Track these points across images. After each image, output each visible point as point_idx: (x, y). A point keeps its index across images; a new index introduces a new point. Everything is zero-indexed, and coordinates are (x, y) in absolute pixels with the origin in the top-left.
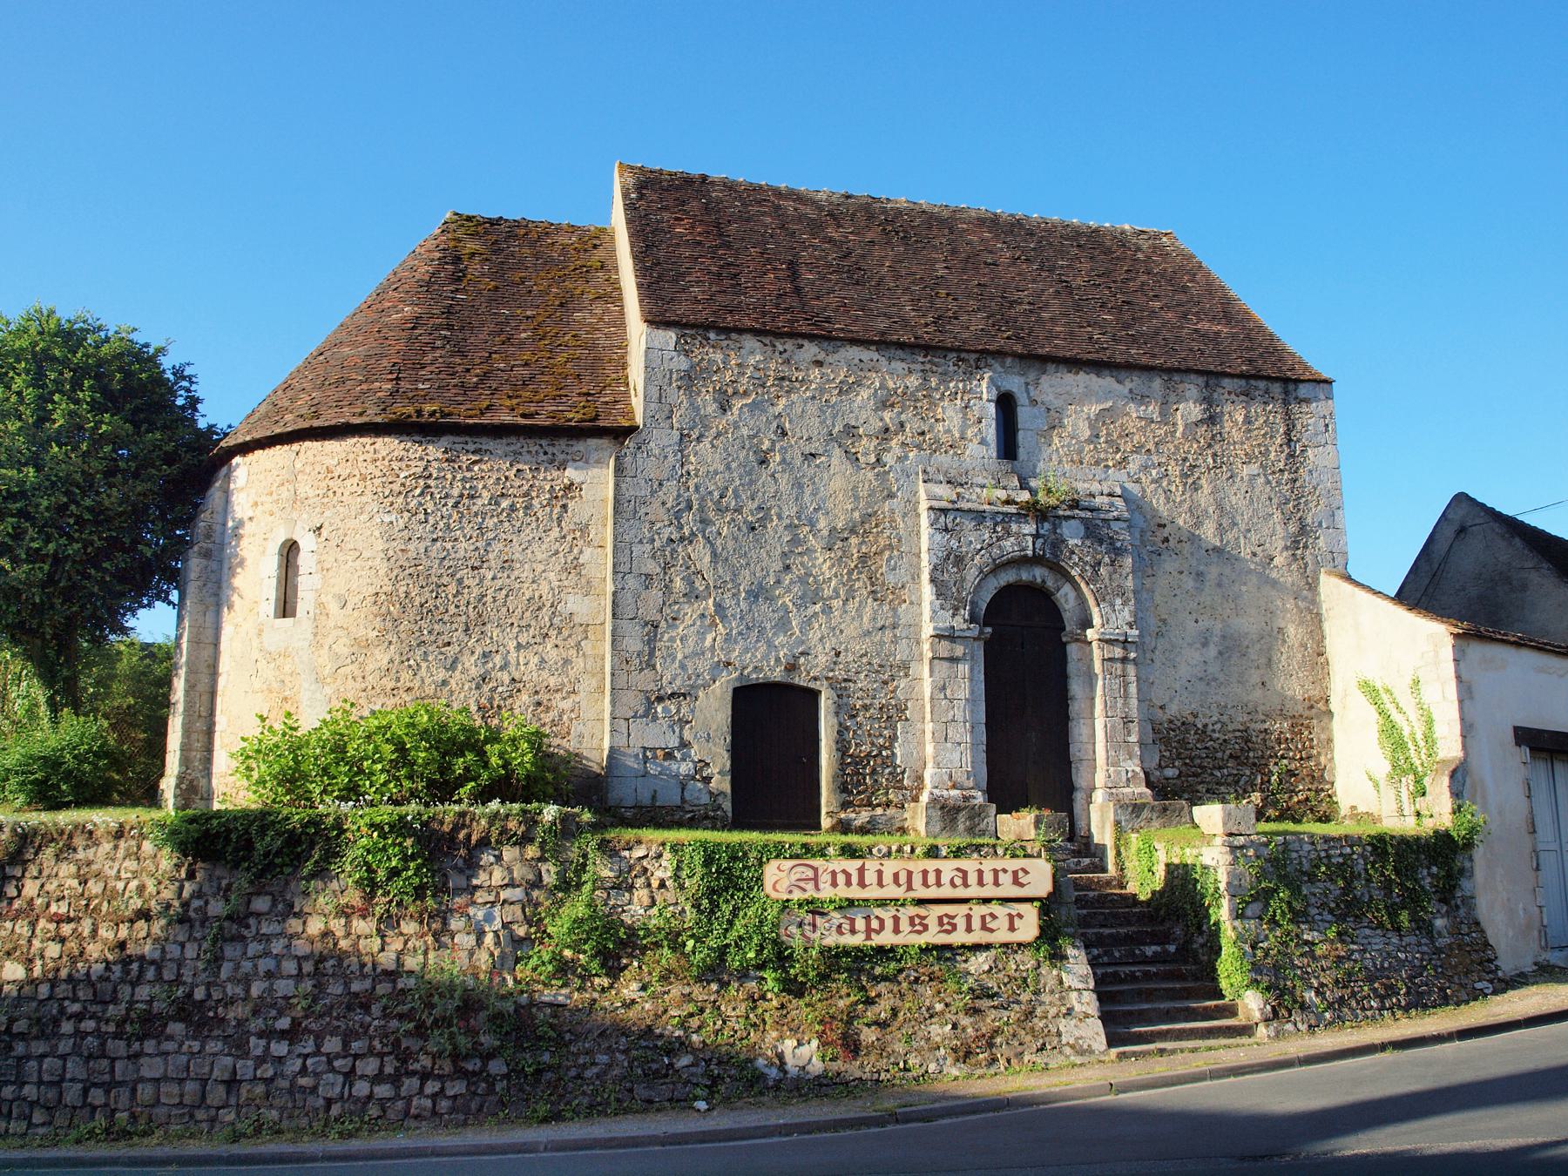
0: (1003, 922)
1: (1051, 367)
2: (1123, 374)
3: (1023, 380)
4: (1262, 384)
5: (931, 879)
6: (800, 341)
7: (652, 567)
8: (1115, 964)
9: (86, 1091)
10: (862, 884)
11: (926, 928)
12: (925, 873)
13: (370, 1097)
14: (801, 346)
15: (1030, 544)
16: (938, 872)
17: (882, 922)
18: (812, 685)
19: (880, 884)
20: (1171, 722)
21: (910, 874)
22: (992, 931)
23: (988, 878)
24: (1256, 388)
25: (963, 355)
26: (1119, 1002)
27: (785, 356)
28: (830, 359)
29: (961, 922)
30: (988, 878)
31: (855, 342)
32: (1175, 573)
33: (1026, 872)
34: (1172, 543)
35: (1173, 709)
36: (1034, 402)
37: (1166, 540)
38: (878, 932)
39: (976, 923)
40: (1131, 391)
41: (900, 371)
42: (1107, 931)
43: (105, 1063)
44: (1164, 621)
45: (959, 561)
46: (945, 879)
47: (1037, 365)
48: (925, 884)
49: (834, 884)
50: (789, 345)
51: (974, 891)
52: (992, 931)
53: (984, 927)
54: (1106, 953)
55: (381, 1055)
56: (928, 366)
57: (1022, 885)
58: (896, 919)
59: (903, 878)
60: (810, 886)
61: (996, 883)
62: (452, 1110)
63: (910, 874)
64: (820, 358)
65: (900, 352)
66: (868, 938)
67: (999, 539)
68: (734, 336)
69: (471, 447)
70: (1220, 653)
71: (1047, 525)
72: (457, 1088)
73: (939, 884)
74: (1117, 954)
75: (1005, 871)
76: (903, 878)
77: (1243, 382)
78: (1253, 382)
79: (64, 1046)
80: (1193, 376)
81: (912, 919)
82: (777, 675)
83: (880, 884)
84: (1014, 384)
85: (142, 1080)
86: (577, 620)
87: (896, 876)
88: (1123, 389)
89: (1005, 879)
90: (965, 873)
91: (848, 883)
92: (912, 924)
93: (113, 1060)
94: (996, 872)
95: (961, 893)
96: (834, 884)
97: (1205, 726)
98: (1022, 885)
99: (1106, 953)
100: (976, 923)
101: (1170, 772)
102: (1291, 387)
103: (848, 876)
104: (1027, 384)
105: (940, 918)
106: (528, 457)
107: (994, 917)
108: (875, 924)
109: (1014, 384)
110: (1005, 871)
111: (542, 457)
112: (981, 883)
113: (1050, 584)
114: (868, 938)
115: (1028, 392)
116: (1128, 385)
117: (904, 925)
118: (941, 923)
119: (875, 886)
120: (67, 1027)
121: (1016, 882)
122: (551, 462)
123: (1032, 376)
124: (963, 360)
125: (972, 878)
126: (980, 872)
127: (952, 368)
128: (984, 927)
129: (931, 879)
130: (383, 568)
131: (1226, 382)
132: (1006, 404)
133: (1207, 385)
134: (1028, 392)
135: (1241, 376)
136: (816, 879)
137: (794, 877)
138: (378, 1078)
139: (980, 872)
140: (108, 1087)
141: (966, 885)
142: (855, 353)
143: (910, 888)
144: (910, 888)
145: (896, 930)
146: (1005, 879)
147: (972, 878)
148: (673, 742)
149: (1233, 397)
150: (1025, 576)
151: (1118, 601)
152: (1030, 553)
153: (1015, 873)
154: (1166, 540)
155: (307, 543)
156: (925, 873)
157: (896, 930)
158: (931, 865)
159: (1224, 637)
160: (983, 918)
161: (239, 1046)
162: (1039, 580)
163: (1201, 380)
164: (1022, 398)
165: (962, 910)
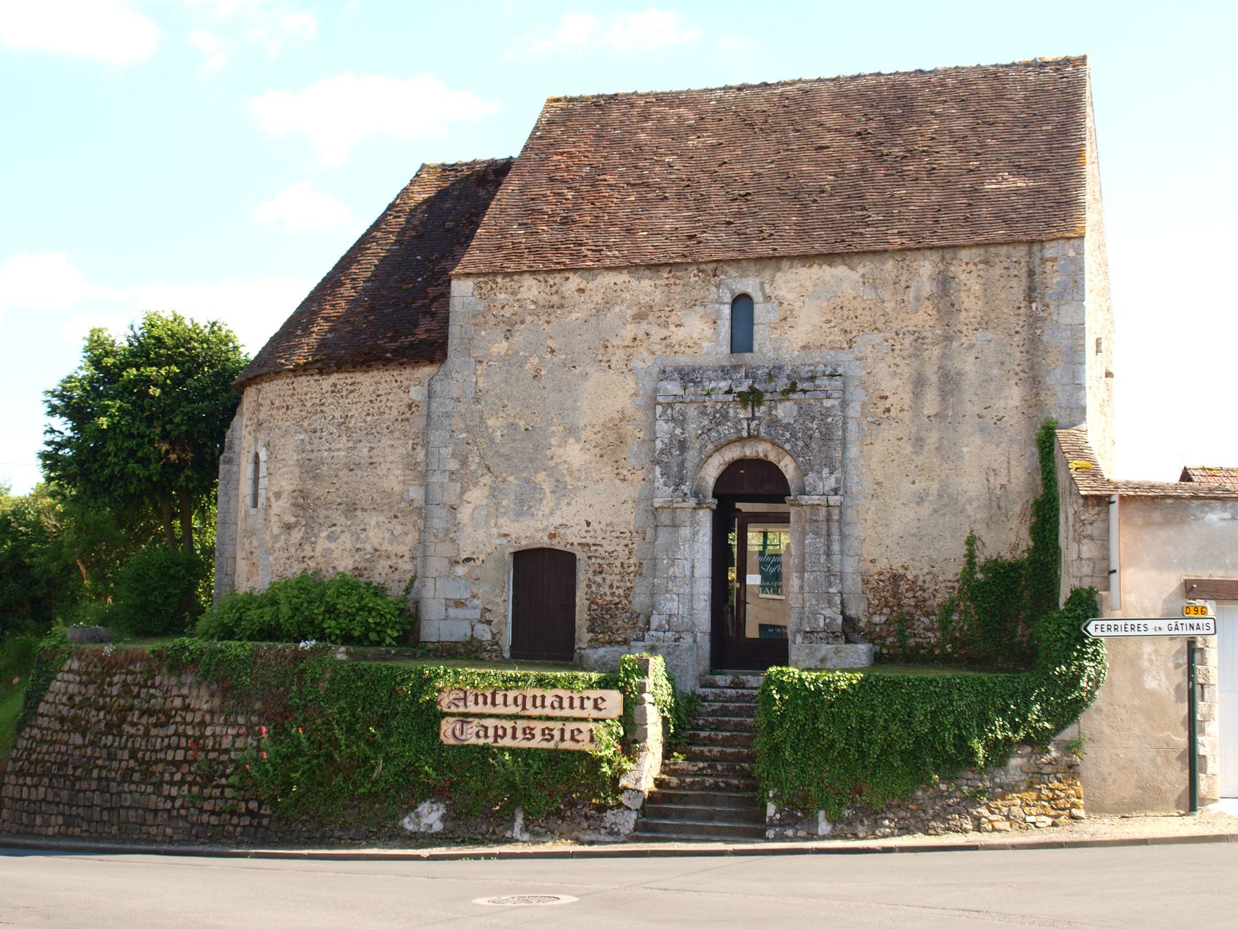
0: (585, 736)
1: (785, 264)
2: (856, 260)
3: (758, 281)
4: (1003, 250)
5: (539, 702)
6: (567, 274)
7: (454, 465)
8: (718, 776)
9: (101, 812)
10: (494, 704)
11: (533, 736)
12: (535, 697)
13: (208, 823)
14: (567, 279)
15: (745, 425)
16: (543, 697)
17: (505, 730)
18: (568, 549)
19: (505, 704)
20: (881, 574)
21: (525, 698)
22: (578, 741)
23: (577, 703)
24: (997, 255)
25: (703, 267)
26: (686, 804)
27: (554, 289)
28: (591, 285)
29: (557, 734)
30: (577, 703)
31: (609, 269)
32: (894, 441)
33: (603, 700)
34: (893, 413)
35: (882, 564)
36: (768, 298)
37: (888, 410)
38: (502, 737)
39: (567, 736)
40: (863, 276)
41: (649, 289)
42: (729, 750)
43: (108, 795)
44: (879, 484)
45: (683, 446)
46: (548, 703)
47: (773, 262)
48: (534, 706)
49: (476, 703)
50: (558, 278)
51: (567, 712)
52: (578, 741)
53: (573, 739)
54: (710, 767)
55: (216, 798)
56: (672, 281)
57: (600, 710)
58: (514, 729)
59: (520, 701)
60: (461, 703)
61: (582, 707)
62: (242, 834)
63: (525, 698)
64: (582, 286)
65: (647, 272)
66: (496, 741)
67: (718, 424)
68: (516, 277)
69: (349, 381)
70: (935, 511)
71: (763, 408)
72: (246, 821)
73: (543, 706)
74: (719, 768)
75: (588, 698)
76: (520, 701)
77: (982, 251)
78: (993, 250)
79: (94, 785)
80: (928, 253)
81: (524, 729)
82: (543, 541)
83: (505, 704)
84: (749, 285)
85: (122, 807)
86: (416, 504)
87: (516, 699)
88: (855, 276)
89: (589, 704)
90: (561, 699)
91: (485, 703)
92: (524, 733)
93: (112, 794)
94: (582, 699)
95: (557, 713)
96: (476, 703)
97: (916, 576)
98: (600, 710)
99: (710, 767)
100: (567, 736)
101: (876, 619)
102: (1036, 248)
103: (485, 698)
104: (762, 284)
105: (543, 730)
106: (385, 385)
107: (580, 731)
108: (500, 732)
109: (749, 285)
110: (588, 698)
111: (395, 385)
112: (571, 707)
113: (772, 458)
114: (496, 741)
115: (762, 289)
116: (861, 270)
117: (519, 734)
118: (543, 734)
119: (502, 706)
120: (95, 773)
121: (596, 707)
122: (400, 387)
123: (767, 274)
124: (703, 271)
125: (566, 703)
126: (571, 699)
127: (693, 279)
128: (573, 739)
129: (539, 702)
130: (297, 471)
131: (965, 254)
132: (742, 303)
133: (943, 258)
134: (762, 289)
135: (977, 245)
136: (465, 699)
137: (452, 697)
138: (213, 812)
139: (571, 699)
140: (110, 809)
141: (561, 707)
142: (609, 279)
143: (524, 708)
144: (524, 708)
145: (514, 737)
146: (589, 704)
147: (566, 703)
148: (466, 595)
149: (971, 267)
150: (749, 451)
151: (826, 471)
152: (745, 434)
153: (596, 700)
154: (888, 410)
155: (263, 456)
156: (535, 697)
157: (514, 737)
158: (539, 692)
159: (940, 496)
160: (572, 731)
161: (158, 786)
162: (761, 455)
163: (935, 256)
164: (757, 297)
165: (559, 725)
